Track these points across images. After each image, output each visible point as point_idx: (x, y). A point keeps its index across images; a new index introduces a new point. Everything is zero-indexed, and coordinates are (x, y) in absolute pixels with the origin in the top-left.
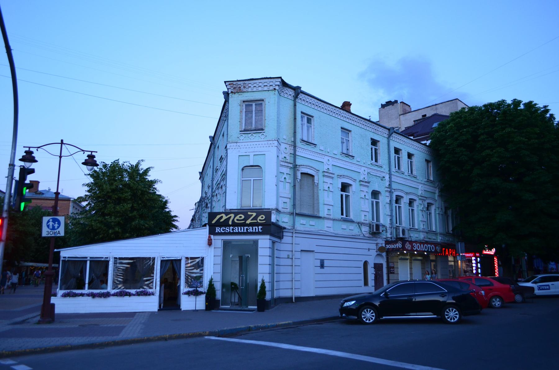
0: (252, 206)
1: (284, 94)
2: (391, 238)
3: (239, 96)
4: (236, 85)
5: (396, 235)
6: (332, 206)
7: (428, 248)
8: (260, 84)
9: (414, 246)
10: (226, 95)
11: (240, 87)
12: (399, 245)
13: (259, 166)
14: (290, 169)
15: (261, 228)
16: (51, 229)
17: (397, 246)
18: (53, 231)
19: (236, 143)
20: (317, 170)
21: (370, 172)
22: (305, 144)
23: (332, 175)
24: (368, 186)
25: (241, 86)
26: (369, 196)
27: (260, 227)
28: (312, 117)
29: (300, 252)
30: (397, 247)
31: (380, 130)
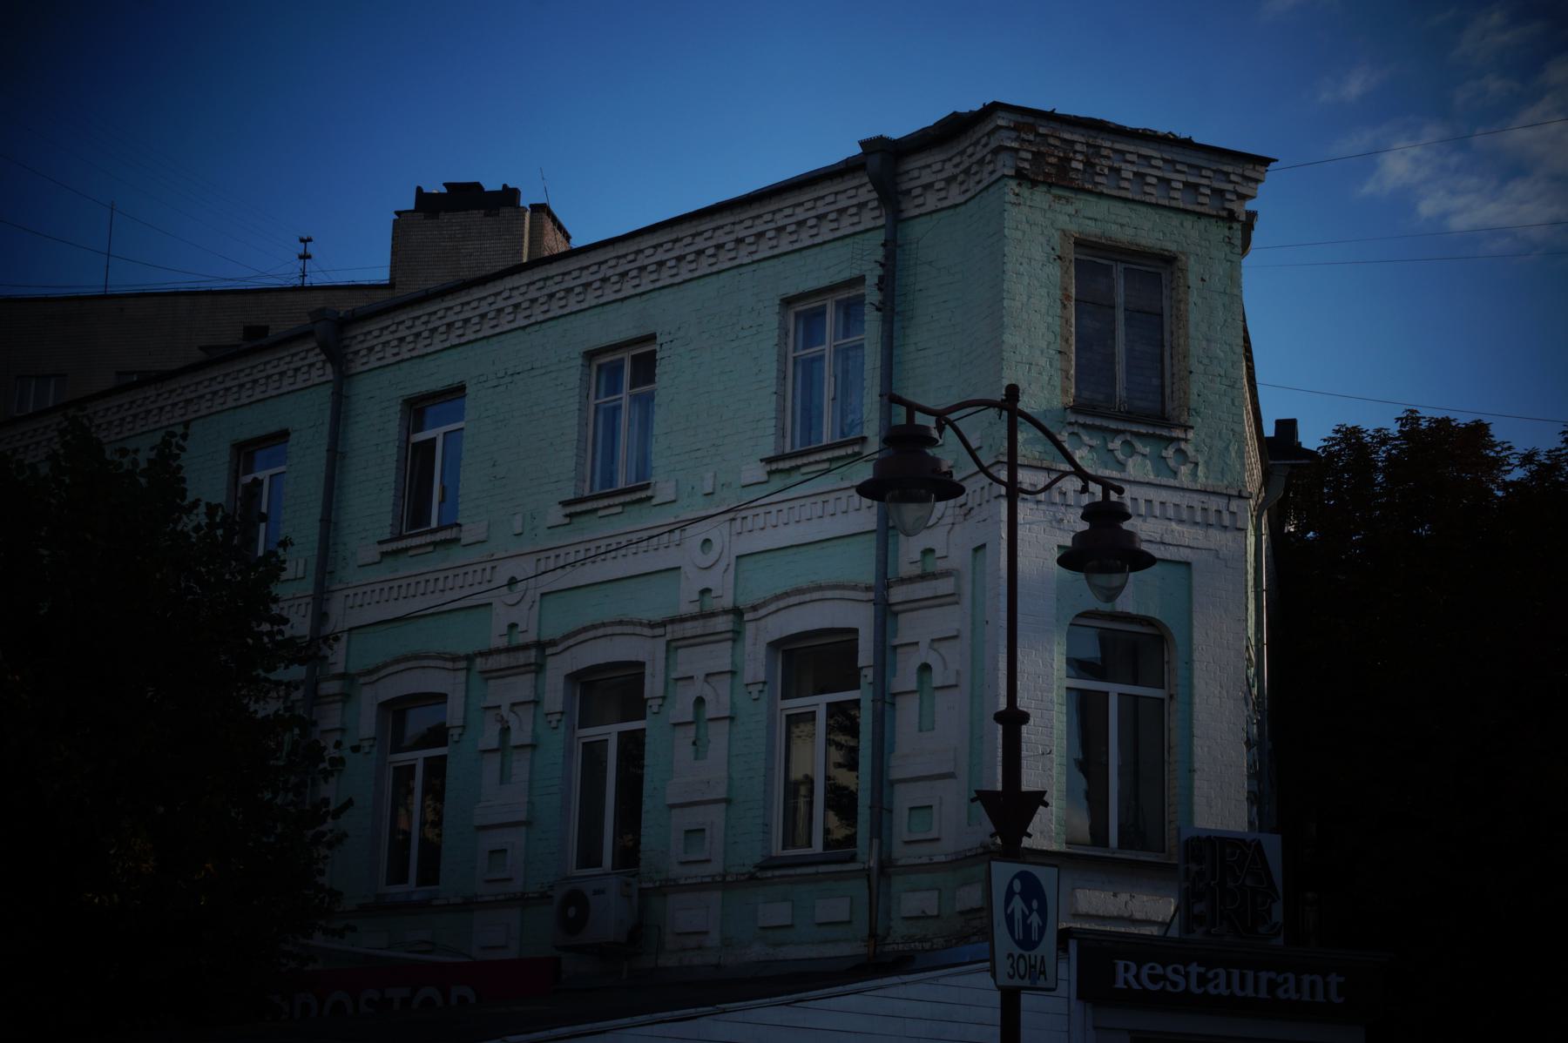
3: (1057, 206)
11: (1064, 164)
16: (1020, 944)
18: (1026, 954)
25: (1071, 155)
27: (1334, 979)
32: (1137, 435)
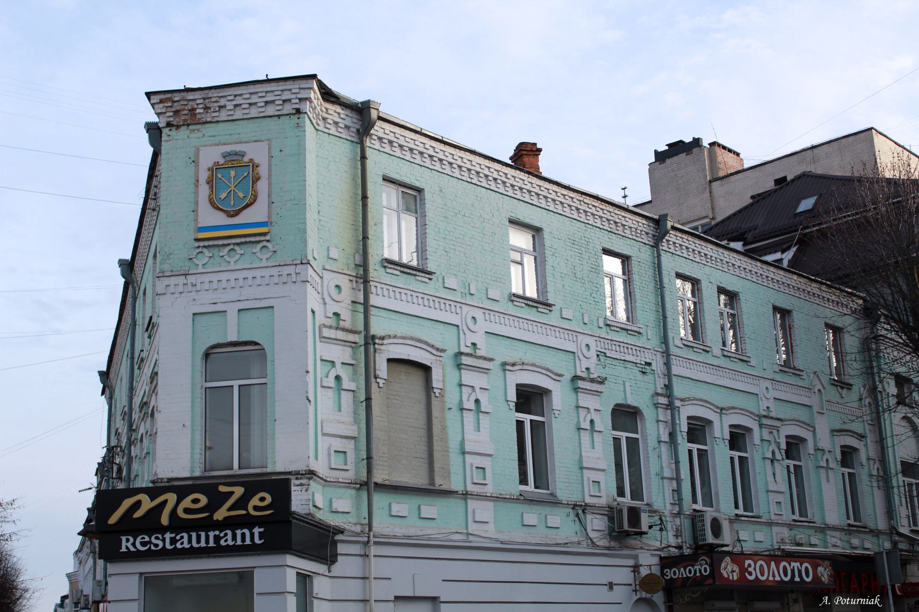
0: (236, 465)
1: (328, 126)
2: (679, 547)
3: (191, 135)
4: (182, 103)
5: (695, 538)
6: (490, 455)
7: (793, 571)
8: (254, 96)
9: (750, 569)
10: (153, 131)
11: (194, 109)
12: (702, 568)
13: (256, 344)
14: (352, 348)
15: (260, 533)
17: (695, 571)
19: (184, 277)
20: (438, 349)
21: (603, 350)
22: (398, 273)
23: (486, 362)
24: (598, 393)
25: (196, 106)
26: (604, 422)
27: (257, 530)
28: (420, 191)
29: (392, 604)
30: (698, 574)
31: (630, 223)
32: (238, 244)
